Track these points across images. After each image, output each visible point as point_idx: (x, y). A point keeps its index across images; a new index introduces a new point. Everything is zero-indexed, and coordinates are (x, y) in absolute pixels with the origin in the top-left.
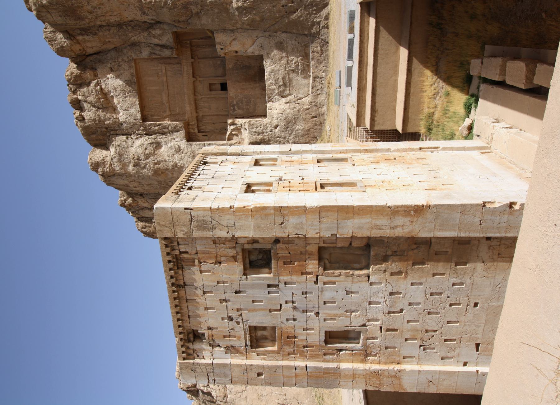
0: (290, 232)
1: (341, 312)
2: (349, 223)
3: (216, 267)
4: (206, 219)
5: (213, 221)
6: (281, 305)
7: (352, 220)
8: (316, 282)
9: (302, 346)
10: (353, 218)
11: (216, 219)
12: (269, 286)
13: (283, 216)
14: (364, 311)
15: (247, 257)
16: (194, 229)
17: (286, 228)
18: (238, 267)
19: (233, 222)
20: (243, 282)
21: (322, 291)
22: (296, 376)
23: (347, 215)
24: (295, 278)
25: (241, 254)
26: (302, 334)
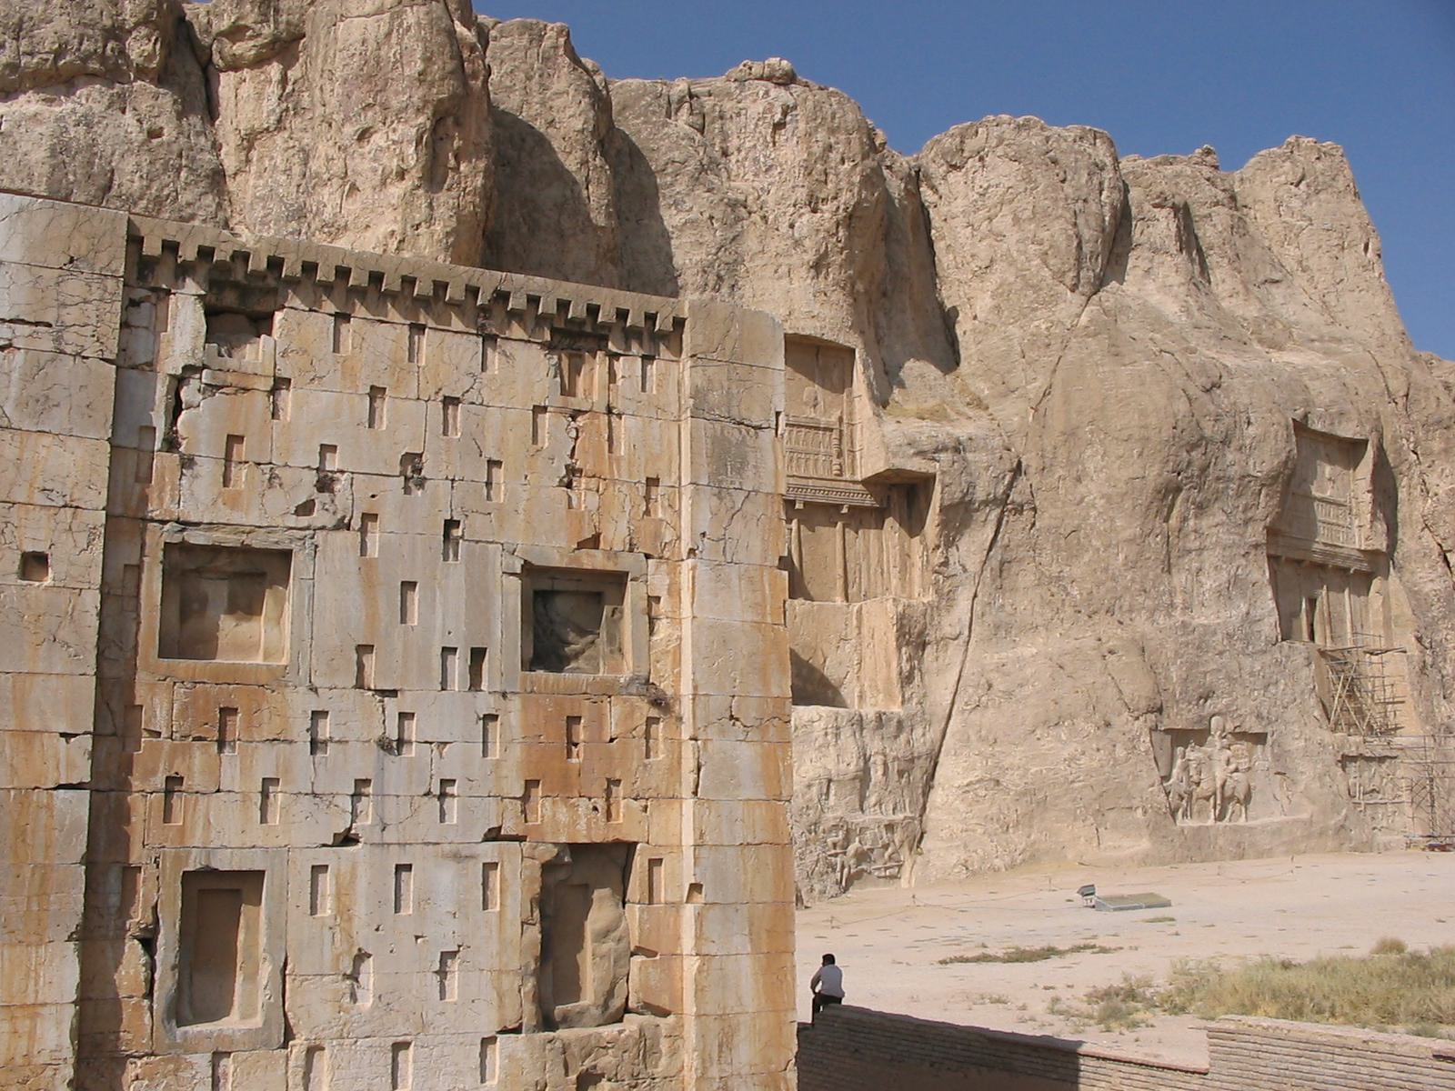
0: (710, 746)
1: (364, 939)
2: (741, 943)
3: (558, 470)
4: (750, 472)
5: (742, 495)
6: (394, 693)
7: (749, 949)
8: (494, 835)
9: (179, 768)
10: (756, 951)
11: (748, 507)
12: (478, 655)
13: (761, 726)
14: (367, 1029)
15: (571, 586)
16: (718, 426)
17: (722, 732)
18: (556, 551)
19: (740, 557)
20: (499, 561)
21: (457, 857)
22: (27, 735)
23: (764, 935)
24: (517, 752)
25: (610, 566)
26: (246, 772)
